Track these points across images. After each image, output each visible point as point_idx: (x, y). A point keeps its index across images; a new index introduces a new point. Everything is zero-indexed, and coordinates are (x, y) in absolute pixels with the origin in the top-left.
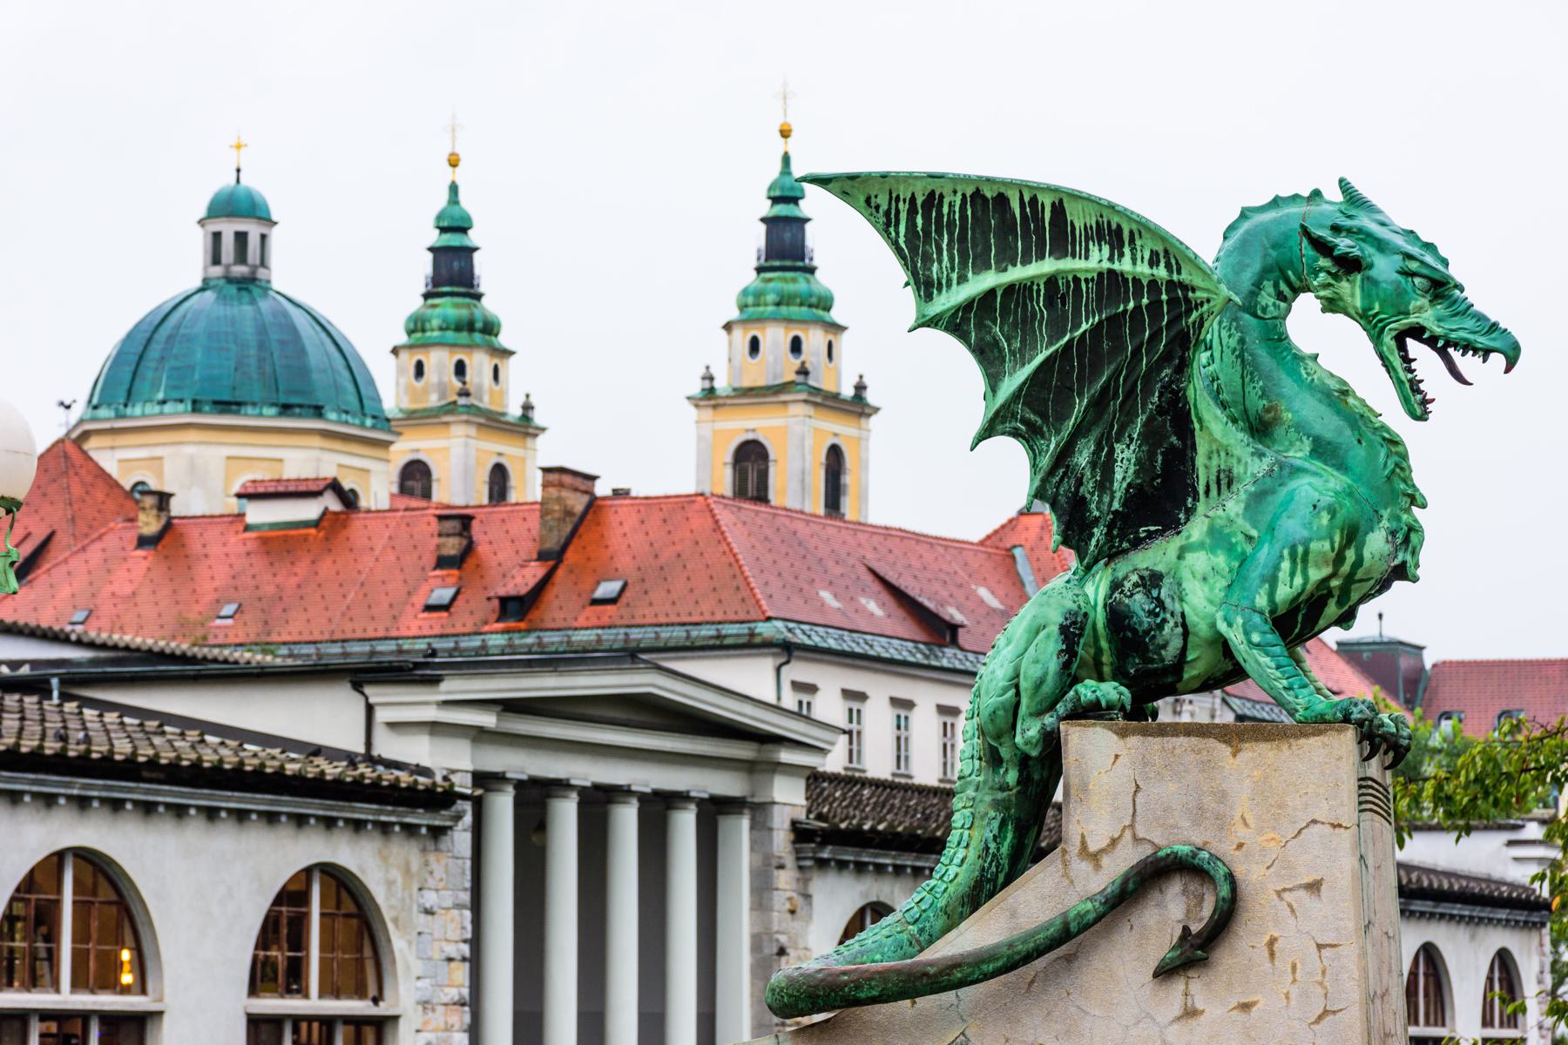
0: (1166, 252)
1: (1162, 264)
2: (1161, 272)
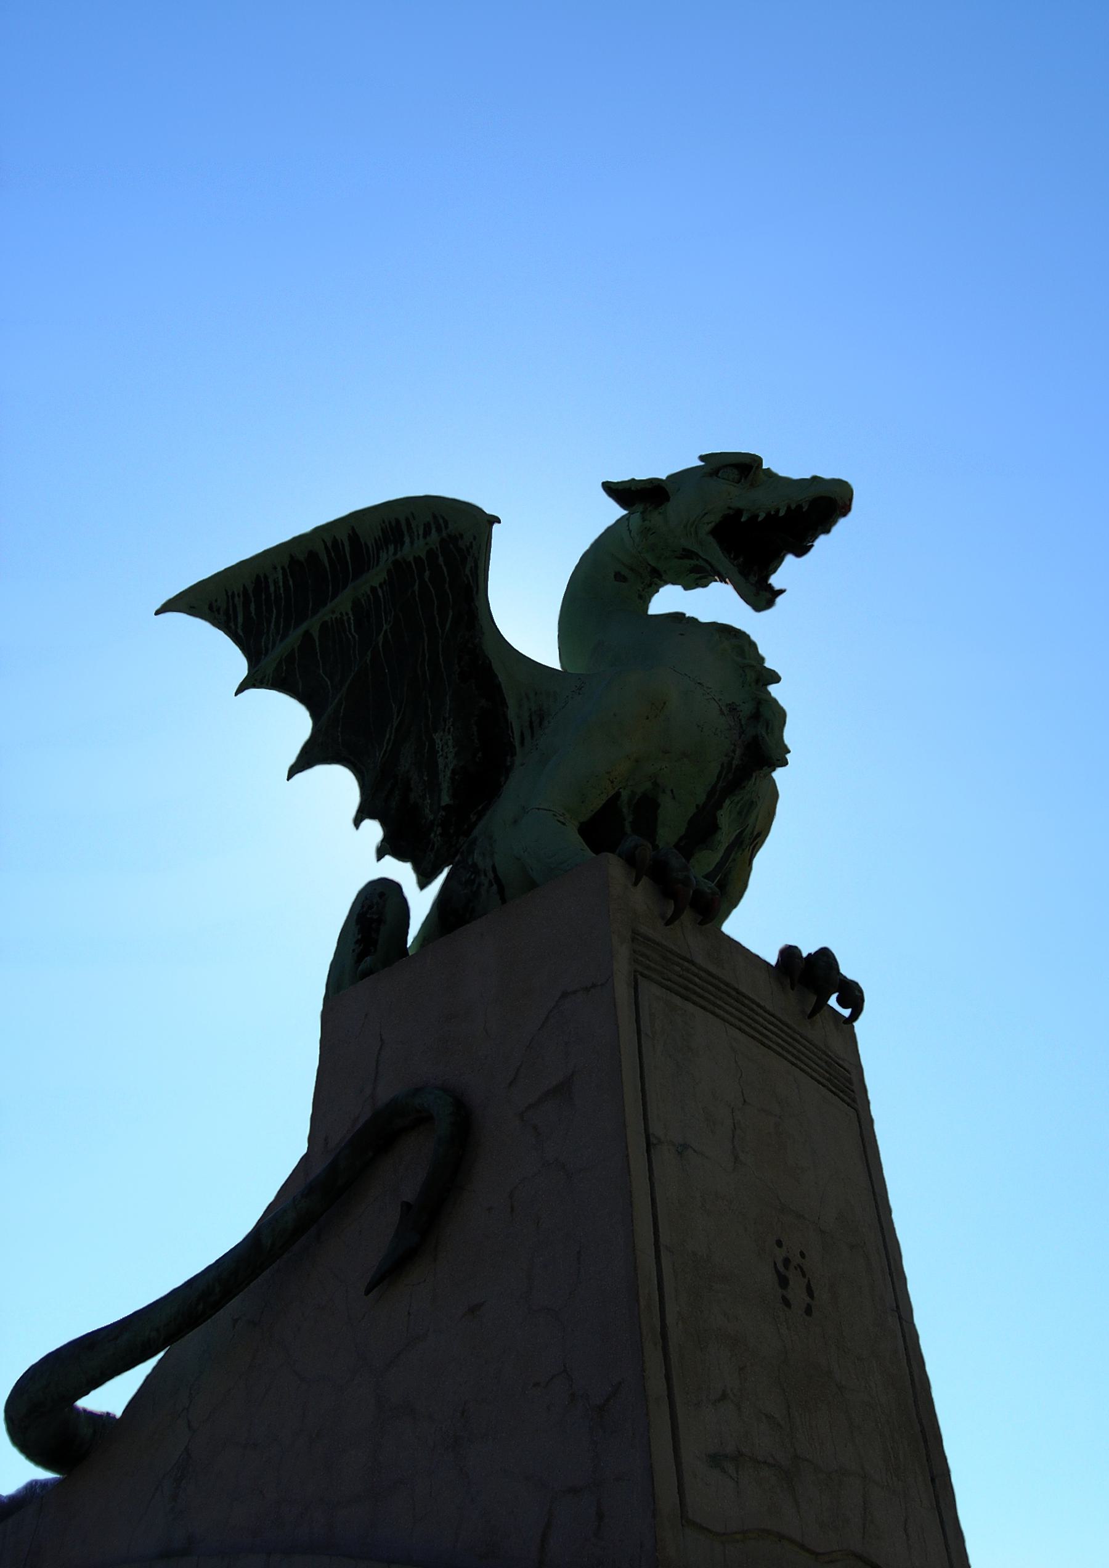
0: (435, 517)
1: (433, 530)
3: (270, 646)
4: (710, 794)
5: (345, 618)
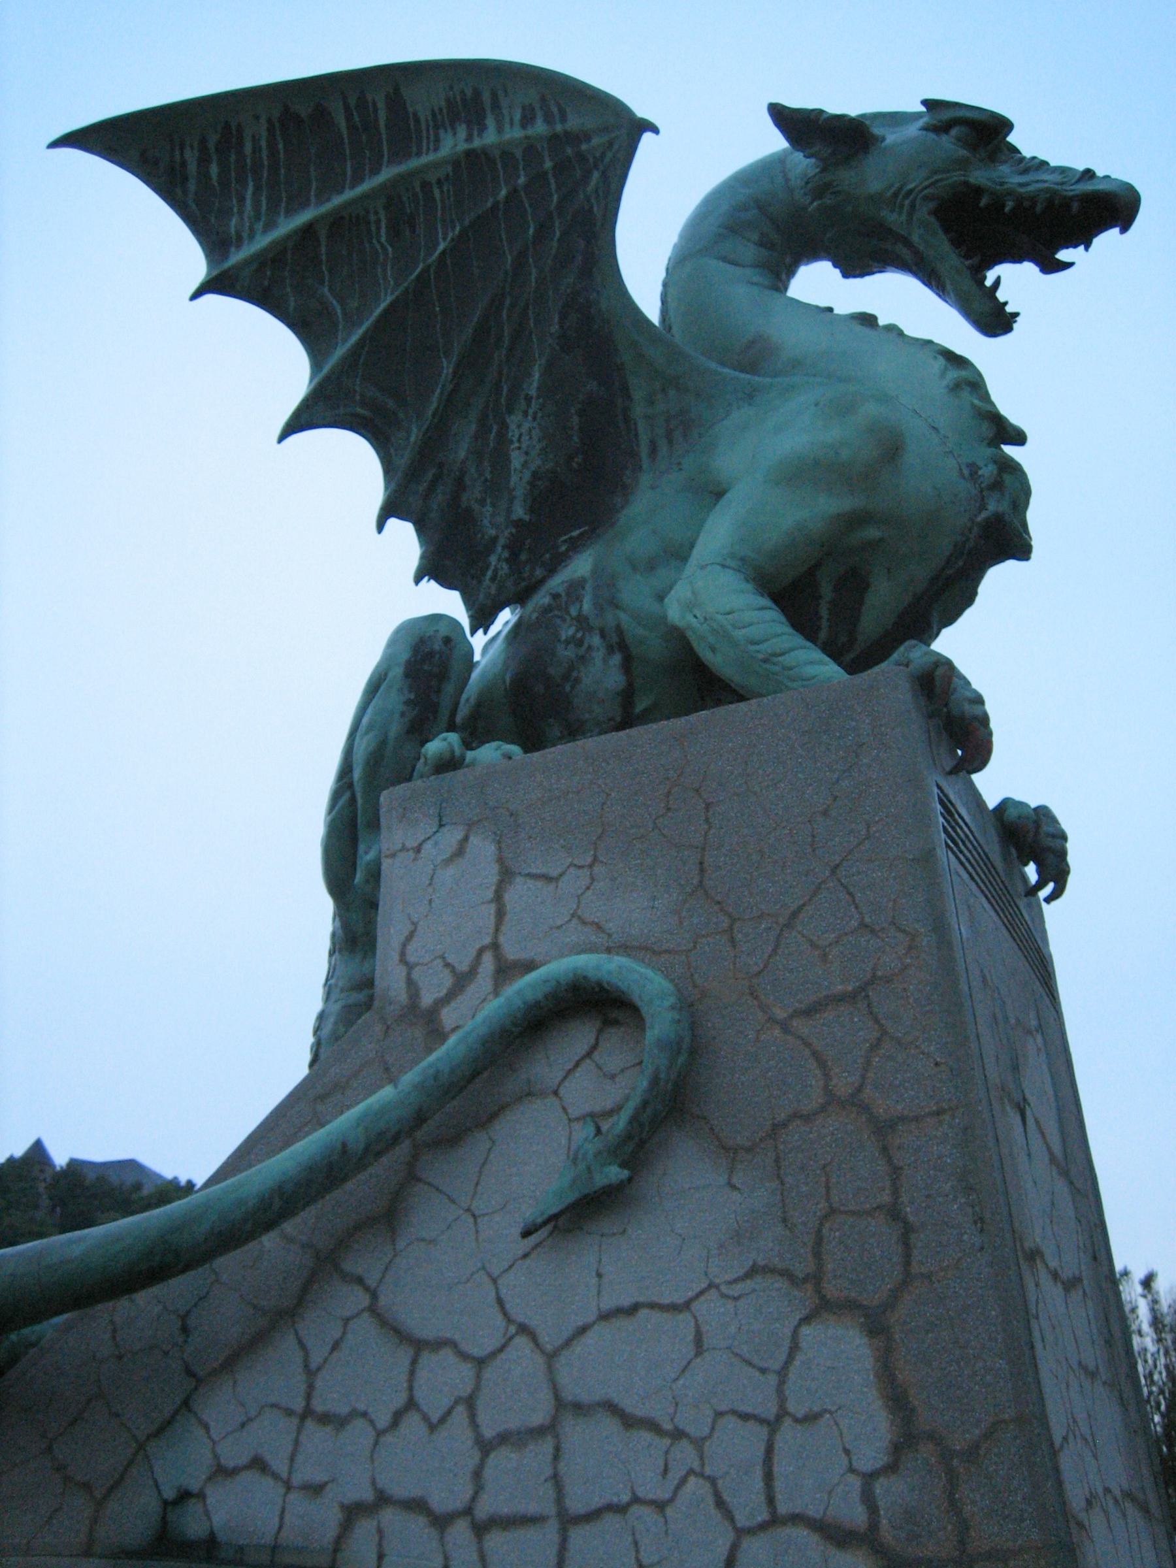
0: (543, 99)
2: (540, 128)
3: (245, 235)
4: (934, 580)
5: (372, 218)
